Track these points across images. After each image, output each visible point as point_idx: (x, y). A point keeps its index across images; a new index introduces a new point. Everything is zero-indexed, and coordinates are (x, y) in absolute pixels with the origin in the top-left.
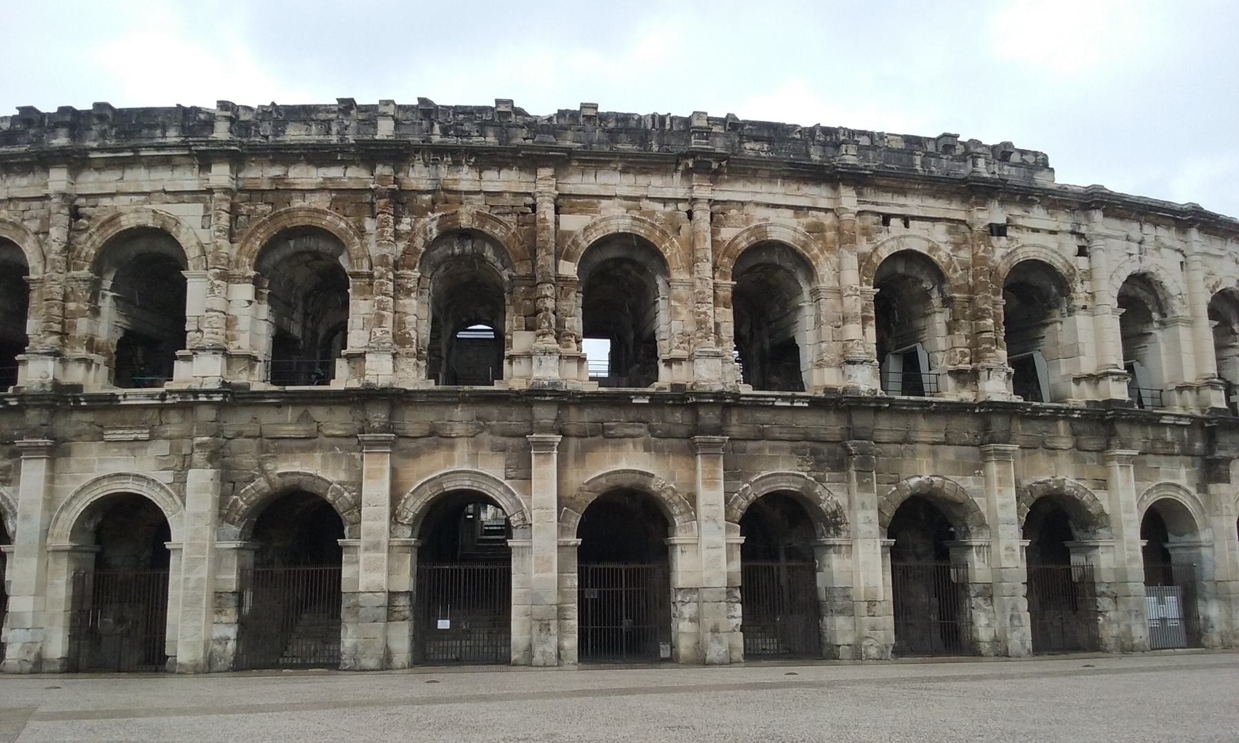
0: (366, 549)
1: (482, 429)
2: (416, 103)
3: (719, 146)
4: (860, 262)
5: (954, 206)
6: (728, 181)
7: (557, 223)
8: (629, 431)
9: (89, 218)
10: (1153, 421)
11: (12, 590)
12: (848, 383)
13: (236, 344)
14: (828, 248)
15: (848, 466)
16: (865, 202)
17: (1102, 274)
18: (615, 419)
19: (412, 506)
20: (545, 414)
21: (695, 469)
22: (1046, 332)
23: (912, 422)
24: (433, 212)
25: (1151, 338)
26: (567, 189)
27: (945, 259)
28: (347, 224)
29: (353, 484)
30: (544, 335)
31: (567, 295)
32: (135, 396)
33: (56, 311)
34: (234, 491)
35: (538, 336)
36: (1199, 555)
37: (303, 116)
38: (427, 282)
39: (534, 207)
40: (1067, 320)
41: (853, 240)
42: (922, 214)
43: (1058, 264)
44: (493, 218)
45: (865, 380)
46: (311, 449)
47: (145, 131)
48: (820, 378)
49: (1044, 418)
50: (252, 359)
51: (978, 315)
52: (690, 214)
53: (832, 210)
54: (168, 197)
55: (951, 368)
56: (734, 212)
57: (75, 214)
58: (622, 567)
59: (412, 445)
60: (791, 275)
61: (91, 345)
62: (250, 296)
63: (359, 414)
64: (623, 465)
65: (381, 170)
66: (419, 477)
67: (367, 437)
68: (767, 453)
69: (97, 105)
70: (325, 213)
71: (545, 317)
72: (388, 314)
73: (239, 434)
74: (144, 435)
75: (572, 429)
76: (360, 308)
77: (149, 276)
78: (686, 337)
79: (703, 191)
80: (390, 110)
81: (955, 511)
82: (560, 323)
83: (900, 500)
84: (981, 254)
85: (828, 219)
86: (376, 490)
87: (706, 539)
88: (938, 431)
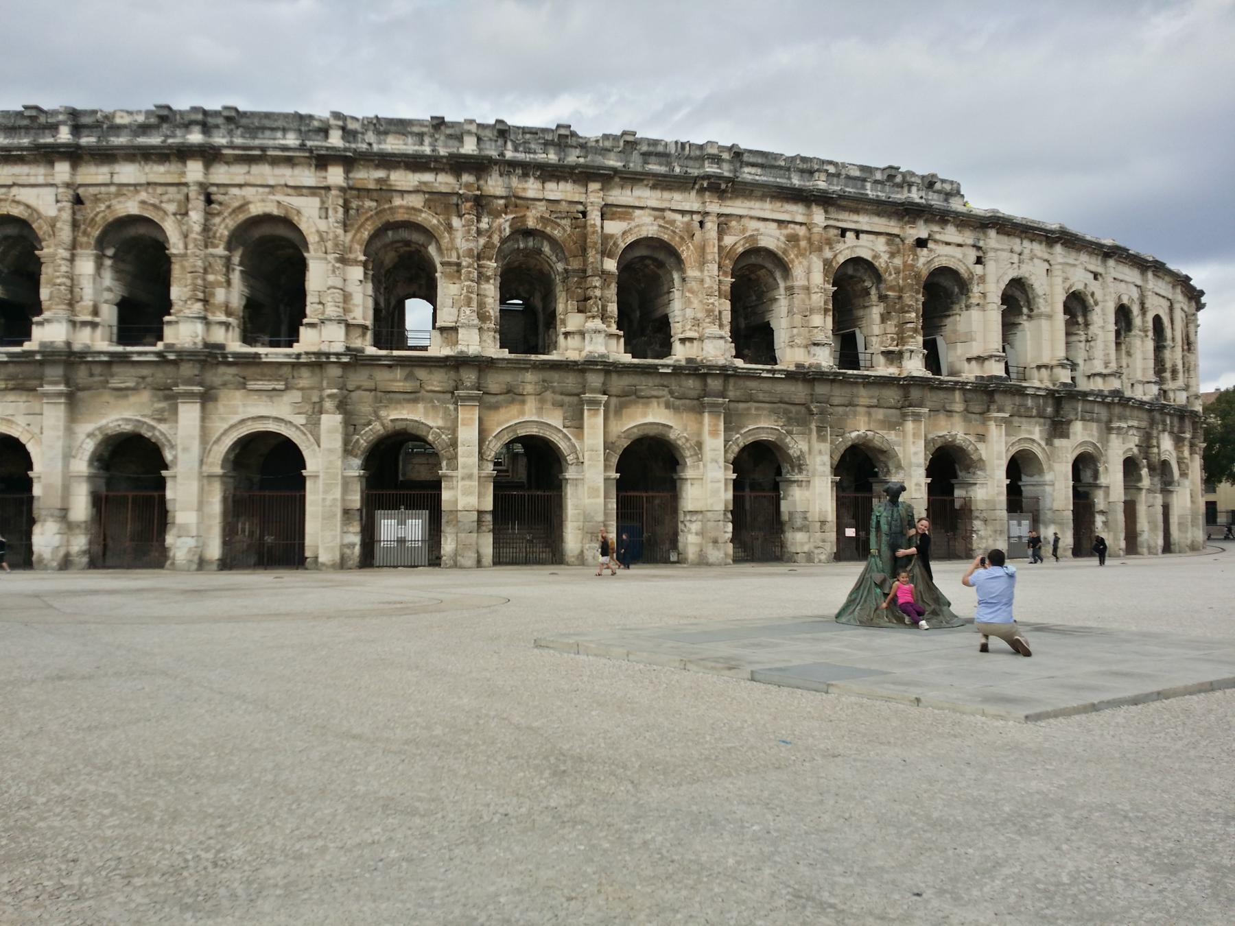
0: (463, 479)
1: (546, 389)
5: (892, 223)
6: (731, 198)
8: (655, 393)
9: (220, 204)
10: (1020, 392)
12: (813, 361)
13: (352, 315)
14: (801, 254)
15: (810, 422)
17: (991, 278)
18: (645, 384)
19: (494, 447)
20: (595, 380)
21: (701, 423)
22: (948, 321)
23: (855, 390)
25: (1020, 327)
26: (610, 200)
27: (883, 265)
29: (448, 429)
30: (594, 317)
33: (200, 282)
34: (355, 431)
36: (1044, 491)
39: (584, 214)
40: (965, 313)
41: (820, 249)
43: (962, 270)
45: (825, 359)
46: (416, 401)
47: (268, 133)
51: (903, 311)
52: (701, 223)
54: (289, 191)
56: (734, 223)
57: (209, 200)
58: (644, 494)
59: (493, 399)
60: (772, 274)
62: (361, 277)
63: (452, 374)
64: (650, 419)
65: (467, 178)
67: (462, 393)
68: (753, 412)
70: (421, 211)
72: (474, 296)
73: (358, 388)
74: (281, 386)
75: (613, 390)
76: (447, 289)
78: (697, 323)
79: (714, 207)
80: (473, 128)
81: (882, 458)
82: (604, 308)
84: (910, 262)
85: (802, 231)
86: (468, 434)
88: (872, 397)
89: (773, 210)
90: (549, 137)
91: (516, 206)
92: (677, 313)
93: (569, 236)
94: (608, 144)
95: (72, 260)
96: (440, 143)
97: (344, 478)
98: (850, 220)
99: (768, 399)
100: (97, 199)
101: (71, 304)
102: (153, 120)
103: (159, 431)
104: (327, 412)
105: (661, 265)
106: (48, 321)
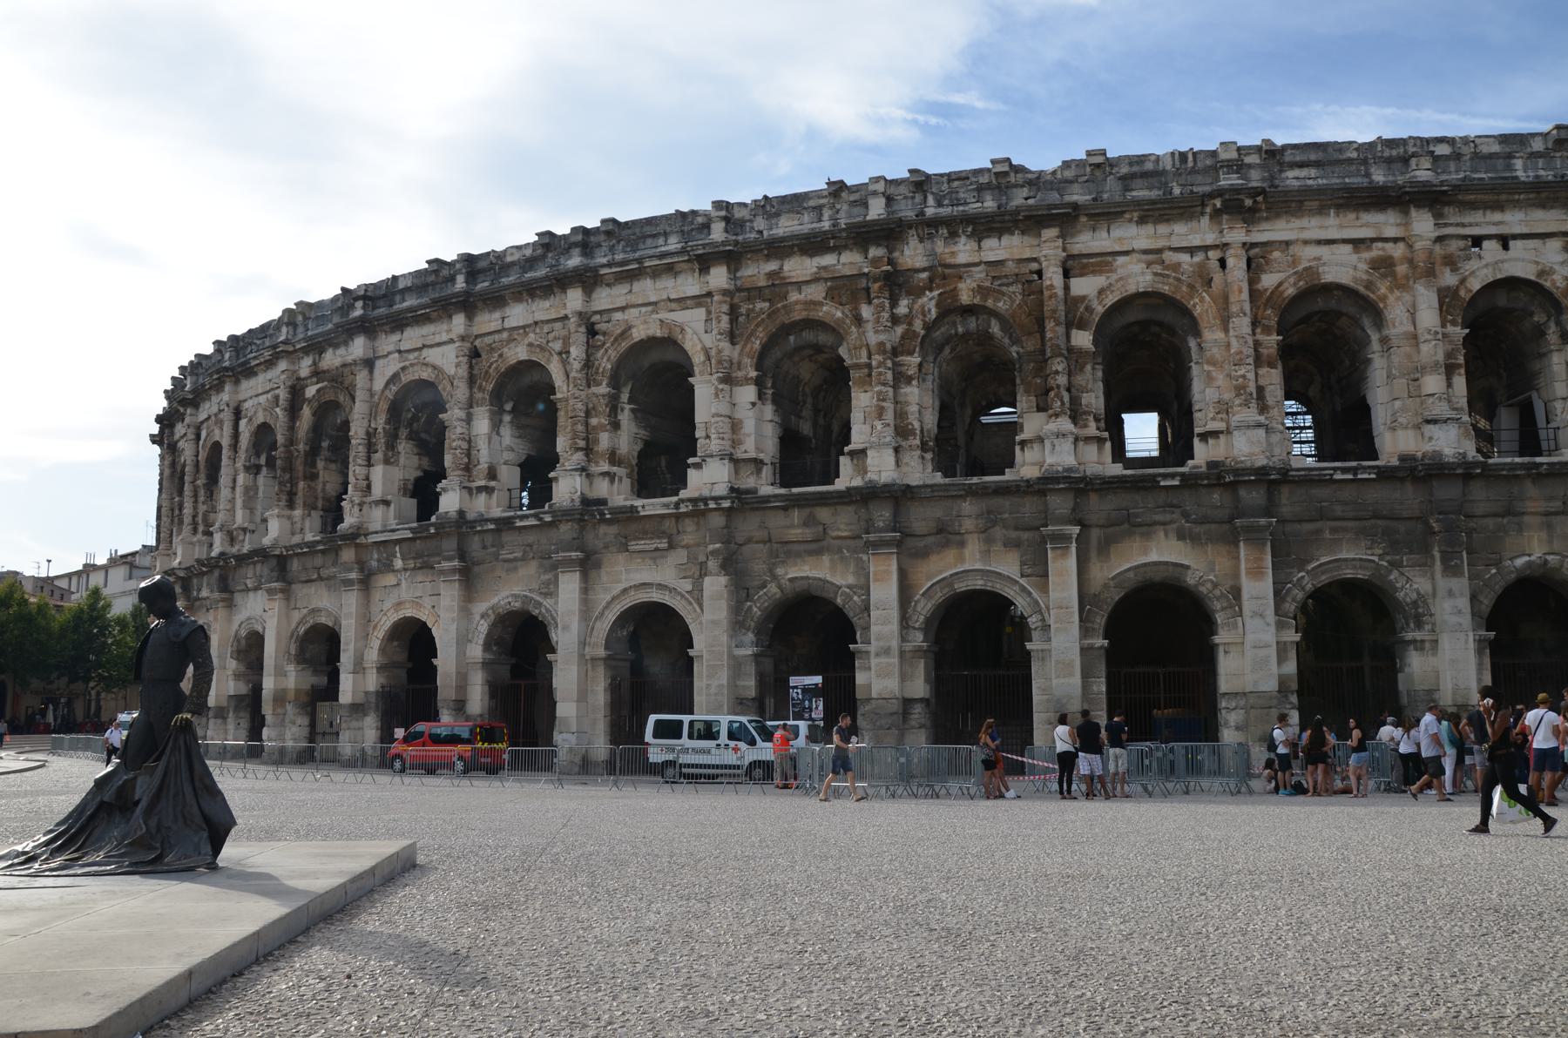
0: (877, 655)
1: (994, 523)
2: (907, 175)
3: (1256, 179)
6: (1267, 219)
7: (1067, 288)
8: (1158, 518)
11: (558, 696)
12: (1428, 447)
13: (743, 448)
14: (1401, 285)
16: (1446, 225)
19: (923, 608)
20: (1060, 504)
21: (1238, 558)
24: (931, 290)
30: (1057, 415)
31: (1082, 369)
32: (653, 506)
33: (580, 427)
34: (748, 597)
39: (1040, 273)
41: (1430, 273)
42: (1525, 230)
45: (1451, 442)
46: (818, 552)
47: (649, 241)
50: (758, 463)
52: (1223, 263)
53: (1403, 239)
54: (674, 305)
56: (1276, 254)
57: (592, 332)
59: (921, 544)
60: (1356, 322)
61: (614, 458)
64: (1154, 557)
65: (874, 252)
67: (872, 537)
68: (1327, 535)
69: (603, 222)
72: (889, 405)
73: (749, 540)
76: (862, 400)
77: (658, 385)
78: (1224, 408)
79: (1237, 235)
80: (880, 187)
83: (1503, 583)
85: (1398, 251)
86: (885, 593)
87: (1250, 638)
88: (1551, 499)
89: (1341, 226)
90: (984, 179)
91: (944, 277)
94: (1069, 174)
95: (469, 419)
96: (842, 214)
97: (731, 656)
98: (1484, 222)
100: (492, 350)
101: (468, 469)
102: (539, 252)
103: (545, 607)
104: (711, 574)
105: (1171, 331)
106: (444, 490)
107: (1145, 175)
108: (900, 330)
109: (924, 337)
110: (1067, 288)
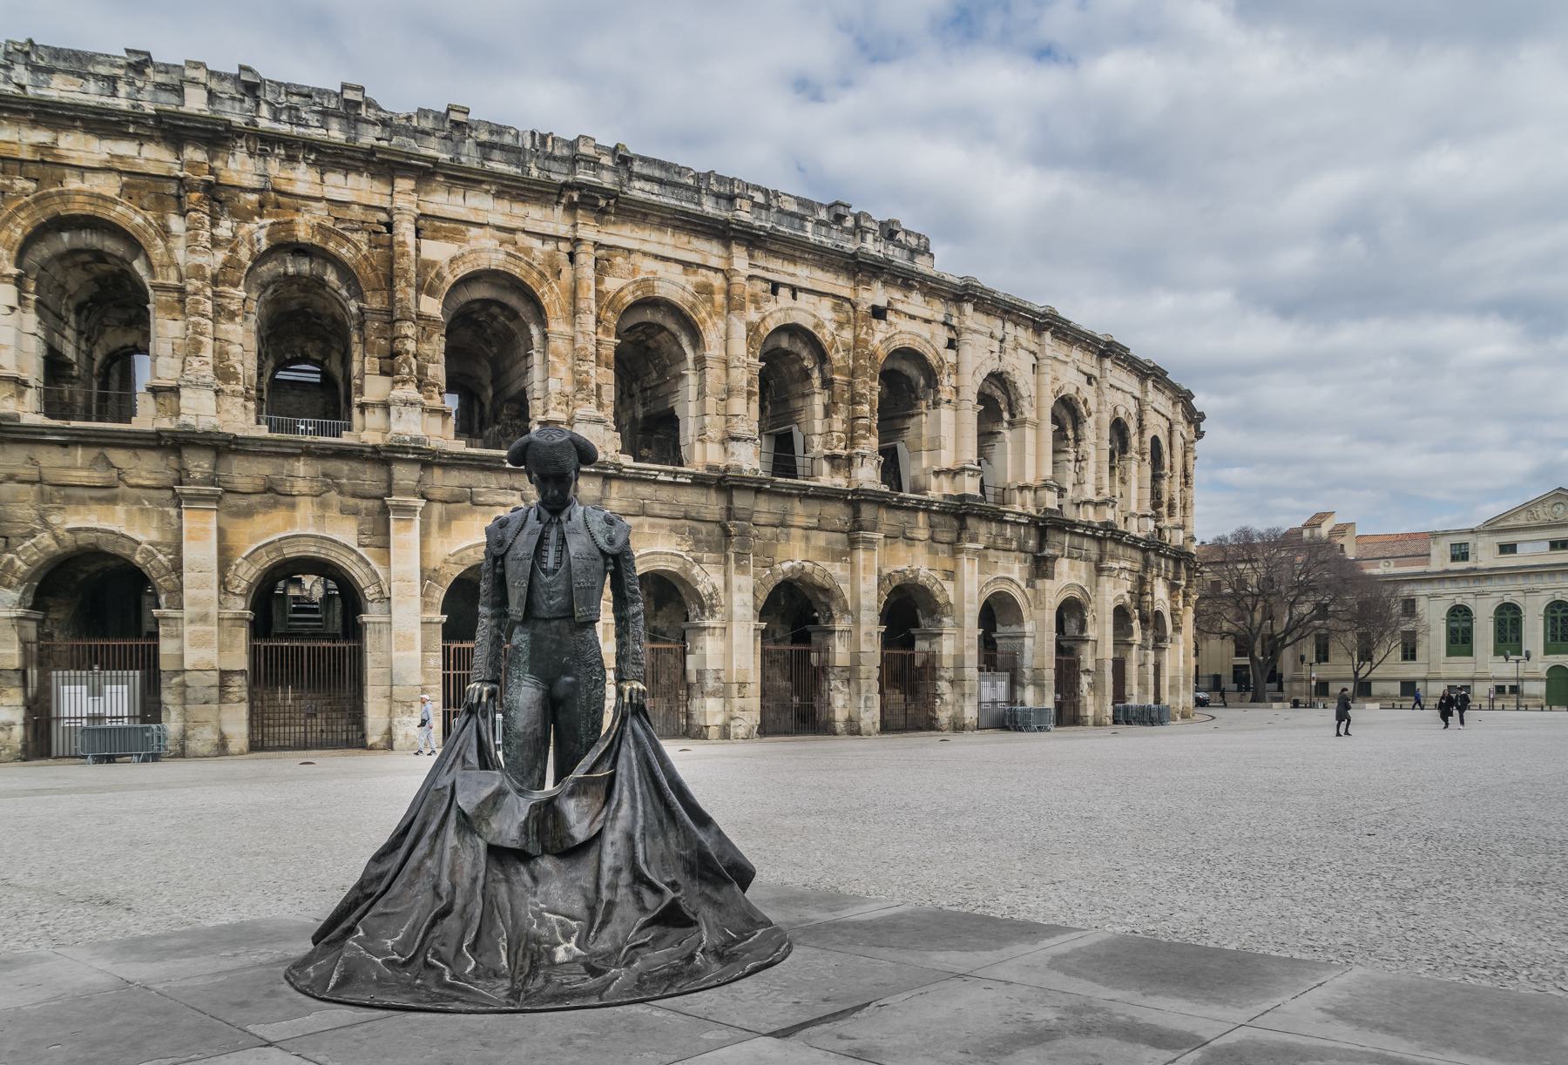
3: (607, 180)
4: (749, 330)
6: (614, 223)
7: (418, 249)
8: (501, 499)
12: (732, 462)
16: (756, 266)
20: (405, 475)
24: (261, 216)
28: (145, 219)
30: (404, 382)
31: (429, 338)
35: (395, 382)
37: (75, 66)
38: (253, 306)
39: (390, 227)
41: (742, 307)
44: (337, 234)
48: (703, 455)
49: (907, 509)
50: (20, 384)
51: (854, 400)
52: (572, 257)
55: (827, 452)
65: (193, 154)
66: (253, 540)
70: (115, 202)
71: (405, 361)
72: (207, 341)
75: (437, 493)
79: (589, 232)
82: (422, 370)
83: (774, 583)
84: (863, 336)
85: (718, 281)
91: (278, 206)
92: (537, 385)
93: (365, 258)
96: (145, 96)
98: (782, 270)
99: (667, 513)
105: (514, 315)
107: (503, 148)
108: (221, 255)
109: (251, 269)
110: (418, 249)
